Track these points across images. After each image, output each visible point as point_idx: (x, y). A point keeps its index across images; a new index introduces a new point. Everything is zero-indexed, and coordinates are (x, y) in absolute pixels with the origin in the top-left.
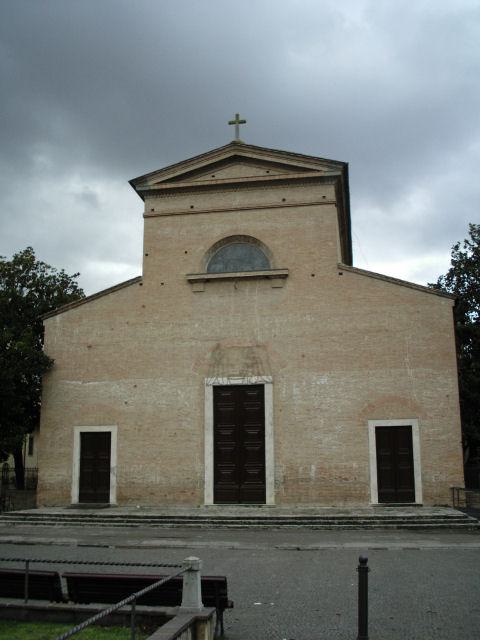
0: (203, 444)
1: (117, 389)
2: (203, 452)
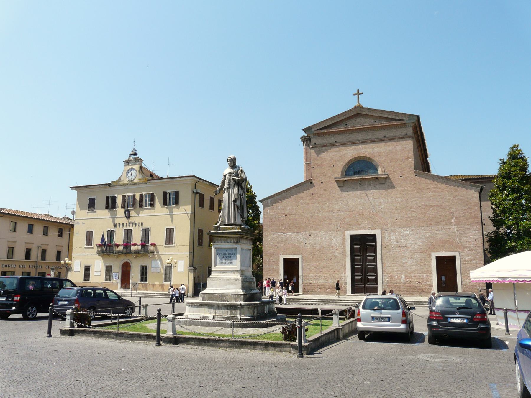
0: (345, 265)
1: (301, 237)
2: (345, 268)
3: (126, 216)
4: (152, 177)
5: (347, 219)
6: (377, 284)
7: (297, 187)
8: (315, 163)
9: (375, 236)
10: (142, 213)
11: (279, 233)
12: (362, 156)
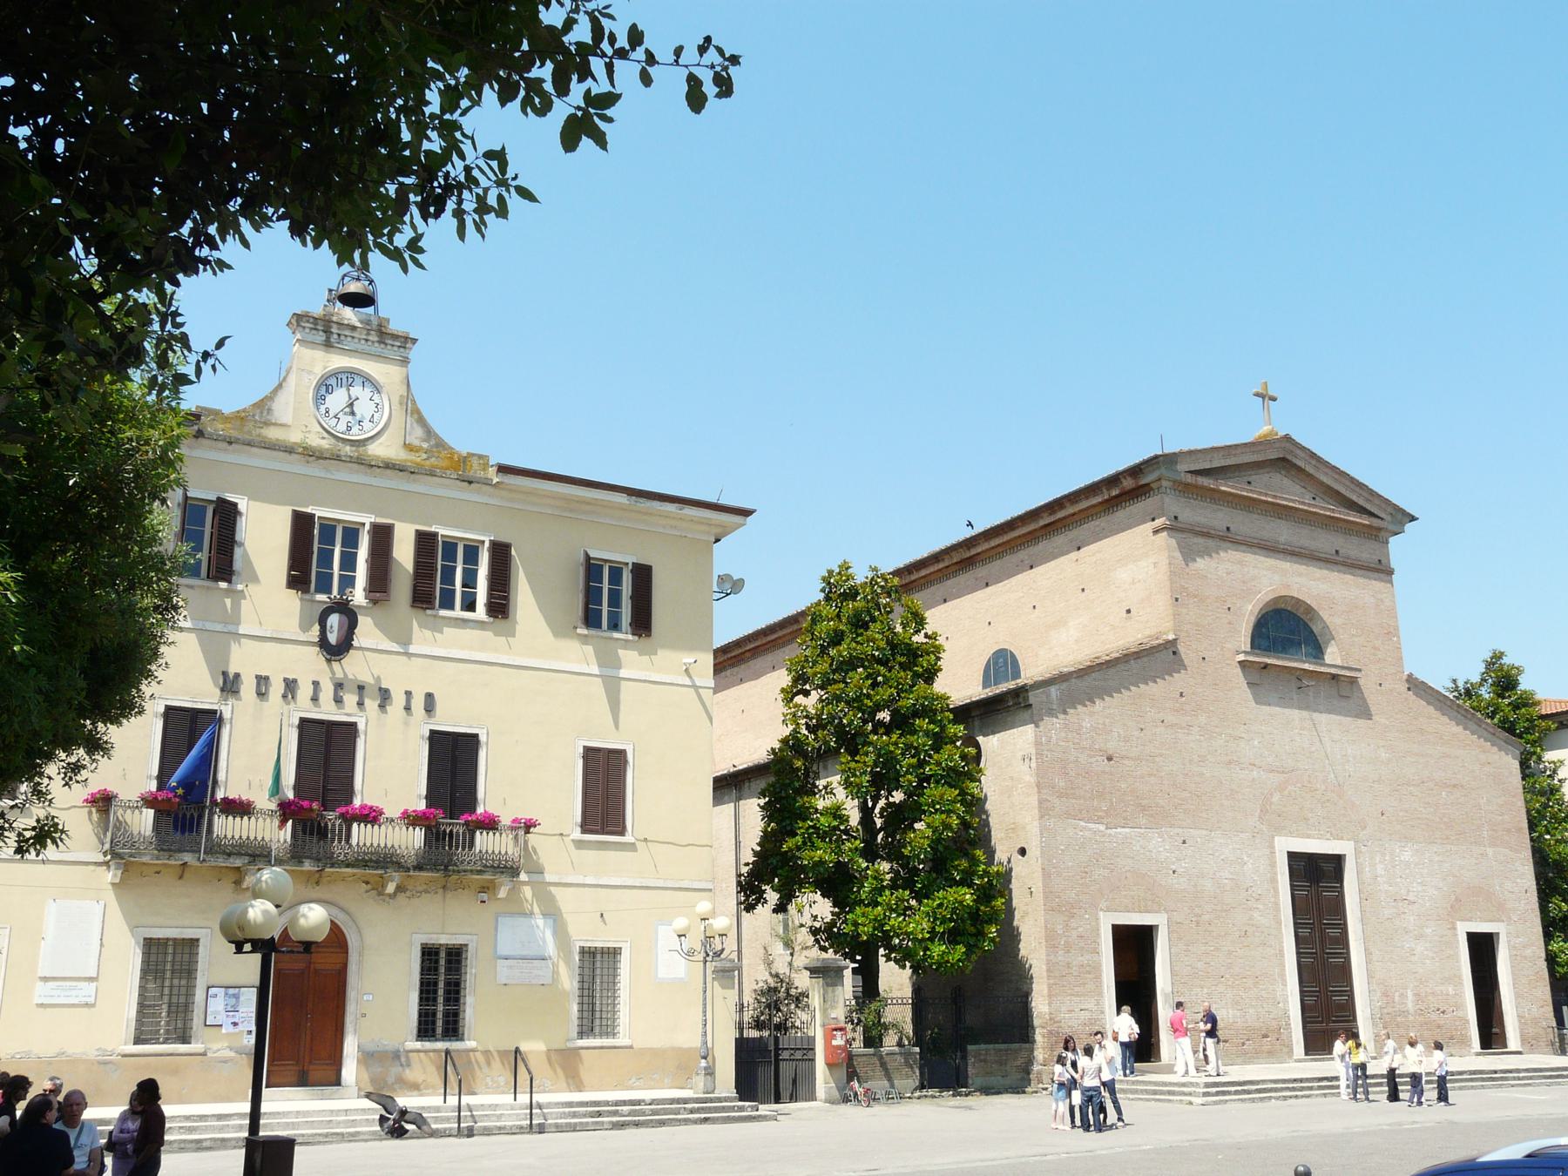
0: (1281, 953)
2: (1282, 965)
3: (323, 643)
4: (441, 444)
5: (1276, 798)
6: (1355, 1019)
7: (1139, 658)
8: (1183, 587)
9: (1337, 861)
10: (424, 640)
11: (1091, 826)
12: (1293, 597)
